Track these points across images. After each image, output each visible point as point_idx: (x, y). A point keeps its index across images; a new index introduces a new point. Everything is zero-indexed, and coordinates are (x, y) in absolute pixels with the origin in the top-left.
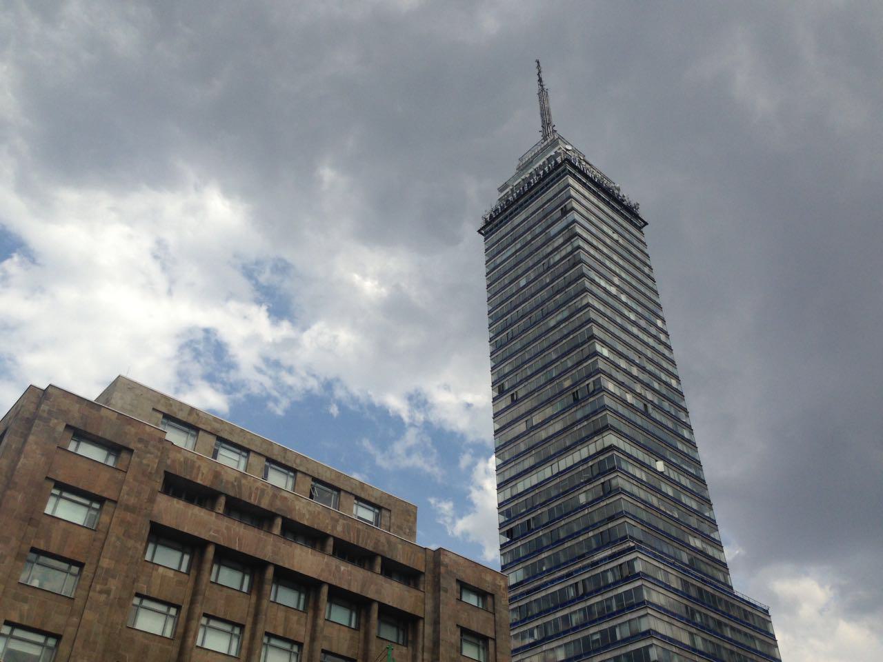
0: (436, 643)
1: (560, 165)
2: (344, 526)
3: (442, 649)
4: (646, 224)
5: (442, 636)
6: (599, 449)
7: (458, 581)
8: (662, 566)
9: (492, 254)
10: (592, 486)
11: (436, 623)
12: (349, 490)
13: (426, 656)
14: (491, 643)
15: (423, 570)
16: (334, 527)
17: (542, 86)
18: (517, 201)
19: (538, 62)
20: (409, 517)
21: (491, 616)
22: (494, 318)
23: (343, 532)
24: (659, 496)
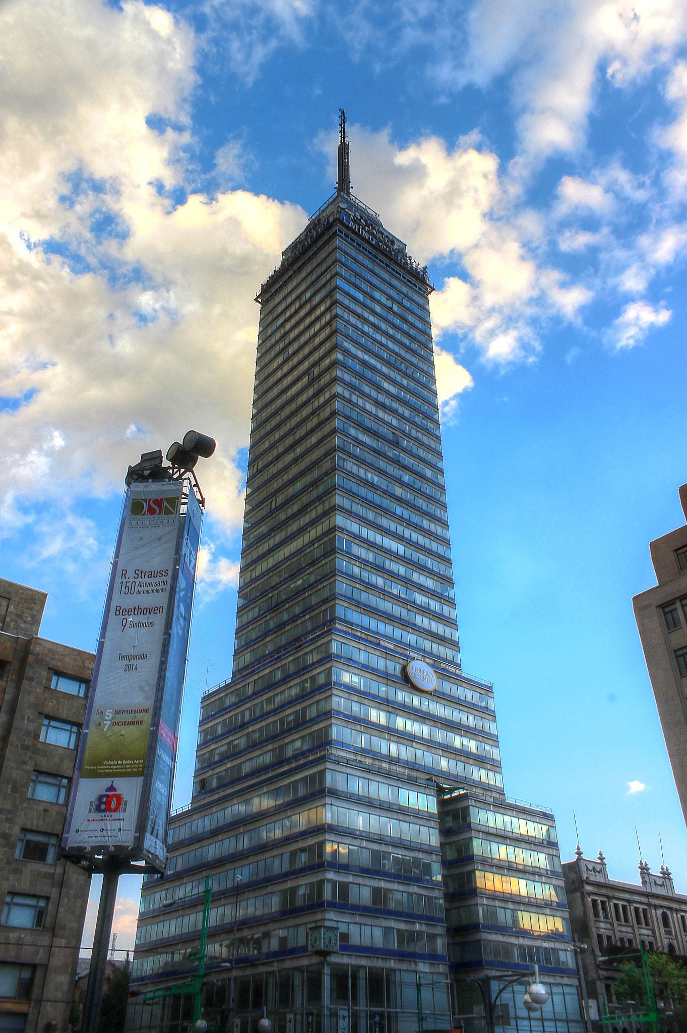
5: (17, 723)
6: (325, 530)
7: (49, 668)
8: (362, 647)
10: (315, 568)
20: (32, 605)
24: (386, 576)
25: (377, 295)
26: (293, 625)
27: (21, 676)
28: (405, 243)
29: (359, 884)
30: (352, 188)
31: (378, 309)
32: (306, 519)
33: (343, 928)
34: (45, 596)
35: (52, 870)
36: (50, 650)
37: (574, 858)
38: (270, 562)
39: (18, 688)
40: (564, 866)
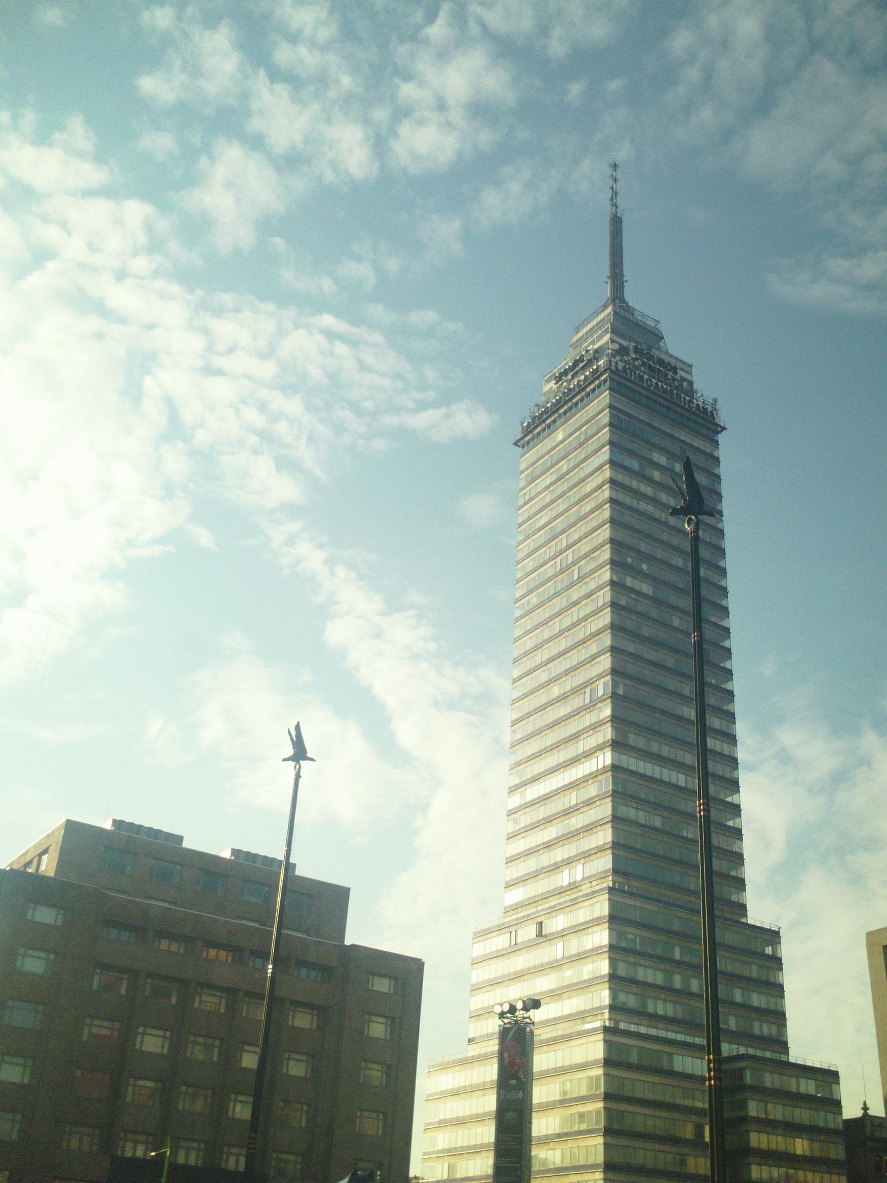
4: (724, 429)
8: (638, 904)
17: (617, 207)
18: (557, 411)
19: (615, 166)
25: (658, 457)
28: (689, 362)
29: (634, 1148)
30: (626, 281)
31: (657, 476)
37: (858, 1113)
40: (847, 1122)
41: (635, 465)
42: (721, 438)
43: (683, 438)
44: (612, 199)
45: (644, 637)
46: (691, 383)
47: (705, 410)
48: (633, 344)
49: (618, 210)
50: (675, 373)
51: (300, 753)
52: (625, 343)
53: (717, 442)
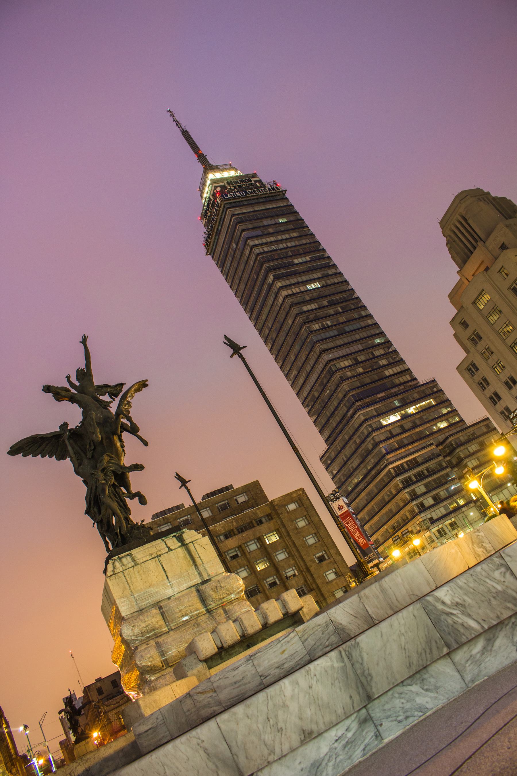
0: (288, 533)
1: (221, 205)
2: (235, 521)
3: (291, 534)
4: (286, 191)
5: (288, 529)
8: (372, 408)
9: (221, 265)
11: (284, 526)
12: (230, 497)
13: (287, 538)
14: (307, 516)
15: (270, 512)
16: (233, 525)
21: (303, 507)
22: (245, 303)
23: (237, 523)
25: (266, 222)
26: (338, 411)
27: (278, 515)
31: (271, 230)
32: (312, 362)
33: (429, 516)
34: (258, 481)
35: (330, 561)
36: (280, 501)
38: (308, 388)
39: (280, 518)
41: (259, 232)
42: (287, 195)
43: (271, 207)
44: (177, 125)
45: (308, 300)
46: (260, 181)
47: (273, 189)
48: (225, 182)
49: (183, 127)
50: (251, 181)
51: (184, 482)
52: (222, 184)
53: (287, 198)
